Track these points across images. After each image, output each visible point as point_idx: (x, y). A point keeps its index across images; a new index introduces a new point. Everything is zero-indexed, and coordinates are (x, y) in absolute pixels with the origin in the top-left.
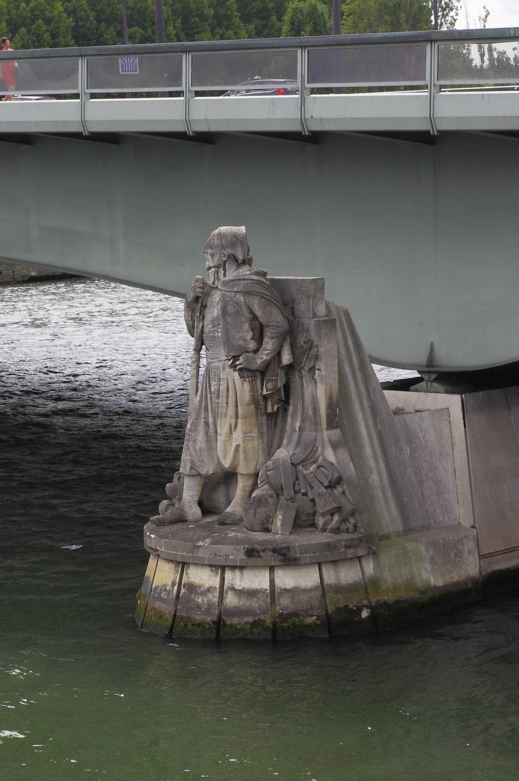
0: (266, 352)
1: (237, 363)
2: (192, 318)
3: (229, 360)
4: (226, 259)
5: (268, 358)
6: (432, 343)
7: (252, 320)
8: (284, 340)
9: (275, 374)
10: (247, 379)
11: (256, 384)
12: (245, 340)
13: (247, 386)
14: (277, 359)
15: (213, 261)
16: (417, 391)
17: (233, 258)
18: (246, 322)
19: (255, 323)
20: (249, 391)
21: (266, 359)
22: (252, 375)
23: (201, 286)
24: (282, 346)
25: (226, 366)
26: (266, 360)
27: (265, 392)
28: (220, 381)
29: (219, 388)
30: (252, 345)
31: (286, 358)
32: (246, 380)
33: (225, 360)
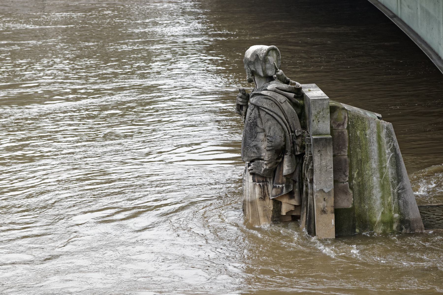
0: (265, 162)
1: (250, 168)
5: (267, 168)
9: (280, 181)
10: (257, 184)
12: (258, 149)
13: (257, 190)
18: (261, 132)
21: (266, 168)
22: (264, 180)
26: (265, 170)
27: (271, 198)
31: (286, 169)
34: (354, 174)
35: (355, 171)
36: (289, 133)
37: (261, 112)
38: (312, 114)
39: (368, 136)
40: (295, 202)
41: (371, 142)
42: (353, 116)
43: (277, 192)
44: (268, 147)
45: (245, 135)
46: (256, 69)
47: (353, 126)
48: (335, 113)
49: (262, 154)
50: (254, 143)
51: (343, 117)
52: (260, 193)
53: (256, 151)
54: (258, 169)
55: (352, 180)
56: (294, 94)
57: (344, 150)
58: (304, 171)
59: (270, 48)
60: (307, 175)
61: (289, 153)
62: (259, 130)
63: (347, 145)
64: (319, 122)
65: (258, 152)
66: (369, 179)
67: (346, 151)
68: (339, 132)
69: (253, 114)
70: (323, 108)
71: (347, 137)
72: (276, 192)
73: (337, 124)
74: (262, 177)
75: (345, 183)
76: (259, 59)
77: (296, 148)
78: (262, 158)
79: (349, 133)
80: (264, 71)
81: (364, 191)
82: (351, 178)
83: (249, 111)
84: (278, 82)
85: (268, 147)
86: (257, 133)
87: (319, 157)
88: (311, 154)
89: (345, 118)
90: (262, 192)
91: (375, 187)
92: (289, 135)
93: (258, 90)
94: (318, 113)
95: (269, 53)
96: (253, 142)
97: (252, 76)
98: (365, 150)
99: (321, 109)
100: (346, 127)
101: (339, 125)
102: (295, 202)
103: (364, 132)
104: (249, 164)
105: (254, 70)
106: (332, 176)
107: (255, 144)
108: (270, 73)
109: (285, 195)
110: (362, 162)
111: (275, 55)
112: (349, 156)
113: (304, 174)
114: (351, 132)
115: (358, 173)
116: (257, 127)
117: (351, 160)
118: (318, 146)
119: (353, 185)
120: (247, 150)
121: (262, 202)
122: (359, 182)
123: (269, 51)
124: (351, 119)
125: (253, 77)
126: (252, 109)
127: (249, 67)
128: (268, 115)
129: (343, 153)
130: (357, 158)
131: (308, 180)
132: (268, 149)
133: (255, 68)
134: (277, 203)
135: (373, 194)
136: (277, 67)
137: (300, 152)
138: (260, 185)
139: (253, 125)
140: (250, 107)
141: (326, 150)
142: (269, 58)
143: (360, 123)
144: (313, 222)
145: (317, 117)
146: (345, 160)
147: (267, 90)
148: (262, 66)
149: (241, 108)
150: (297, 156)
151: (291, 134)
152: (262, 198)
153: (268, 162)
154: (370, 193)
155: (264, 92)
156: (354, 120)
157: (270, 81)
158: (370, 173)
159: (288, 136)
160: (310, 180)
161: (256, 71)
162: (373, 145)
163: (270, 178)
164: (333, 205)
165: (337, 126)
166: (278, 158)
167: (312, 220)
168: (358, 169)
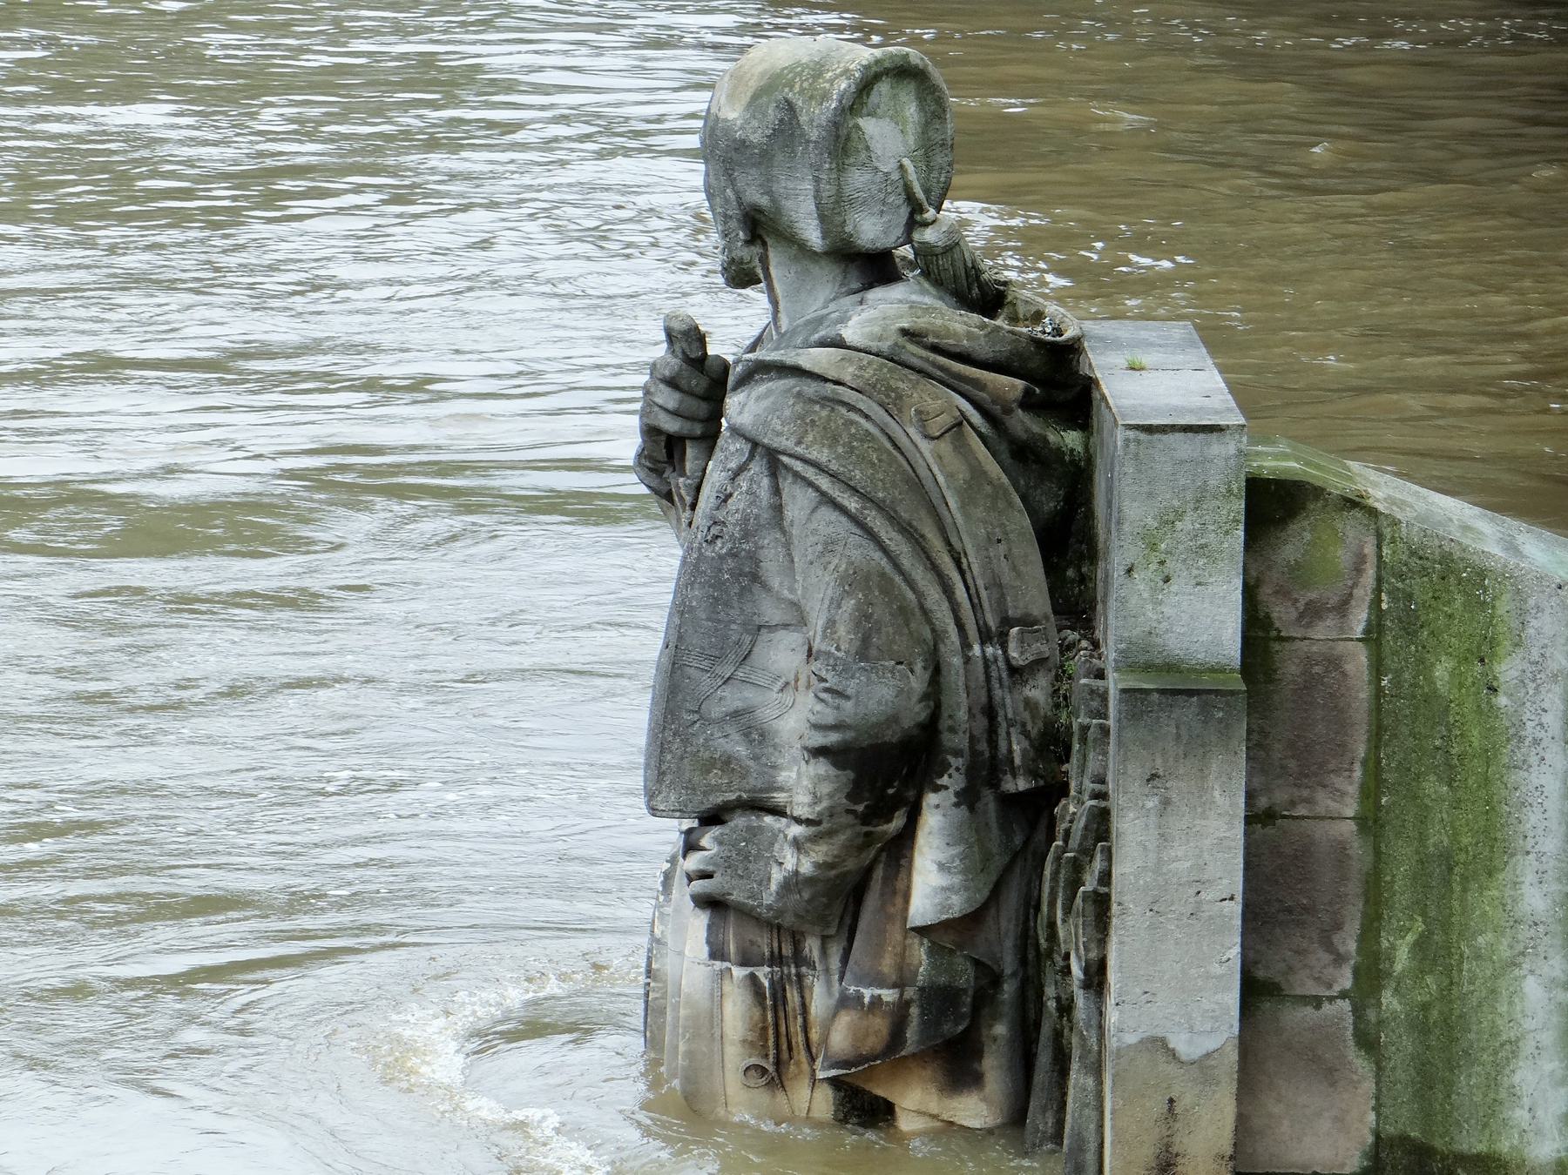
0: (796, 830)
1: (693, 862)
5: (806, 868)
9: (887, 965)
10: (739, 972)
12: (757, 734)
13: (736, 1012)
18: (786, 626)
20: (744, 1041)
21: (796, 873)
22: (787, 950)
26: (793, 883)
34: (1393, 947)
35: (1403, 931)
36: (966, 645)
37: (787, 484)
38: (1126, 527)
39: (1502, 700)
41: (1521, 740)
42: (1413, 553)
43: (867, 1035)
44: (816, 727)
45: (680, 638)
46: (773, 200)
47: (1410, 626)
48: (1294, 527)
50: (733, 698)
51: (1343, 557)
53: (741, 750)
54: (746, 876)
55: (1376, 990)
56: (1020, 384)
57: (1338, 781)
58: (1052, 904)
59: (877, 62)
60: (1072, 934)
61: (953, 781)
62: (771, 612)
63: (1361, 751)
64: (1167, 580)
65: (756, 758)
66: (1493, 991)
67: (1352, 789)
68: (1309, 660)
69: (737, 503)
70: (1204, 488)
71: (1363, 695)
72: (858, 1036)
73: (1301, 605)
74: (773, 926)
75: (1326, 1007)
76: (803, 135)
77: (1010, 751)
79: (1377, 668)
81: (1451, 1071)
82: (1371, 975)
83: (716, 476)
84: (923, 292)
85: (816, 727)
87: (1153, 819)
88: (1102, 796)
89: (1358, 569)
90: (764, 1029)
91: (1528, 1047)
92: (967, 660)
93: (785, 339)
94: (1168, 521)
95: (874, 98)
96: (726, 692)
97: (749, 242)
98: (1482, 793)
99: (1189, 496)
100: (1358, 630)
101: (1313, 612)
102: (983, 1108)
103: (1478, 668)
104: (689, 832)
105: (764, 201)
106: (1237, 949)
107: (739, 704)
108: (871, 230)
109: (914, 1055)
110: (1450, 869)
111: (911, 111)
112: (1370, 823)
113: (1052, 925)
114: (1391, 663)
115: (1420, 946)
116: (756, 588)
117: (1377, 853)
118: (1145, 746)
119: (1380, 1022)
120: (686, 742)
121: (763, 1097)
122: (1425, 1007)
123: (868, 82)
124: (1401, 577)
125: (756, 250)
126: (733, 465)
127: (732, 181)
129: (1325, 803)
130: (1422, 838)
132: (818, 739)
133: (769, 193)
135: (1513, 1094)
136: (920, 194)
137: (1033, 773)
138: (753, 978)
139: (737, 574)
140: (730, 450)
141: (1202, 774)
142: (868, 125)
143: (1458, 604)
145: (1153, 547)
146: (1341, 848)
147: (839, 343)
148: (817, 180)
149: (670, 455)
150: (1009, 802)
151: (977, 649)
152: (764, 1071)
154: (1493, 1082)
156: (1417, 585)
157: (869, 286)
158: (1504, 951)
159: (957, 661)
160: (1086, 971)
161: (778, 210)
162: (1533, 760)
164: (1229, 1151)
165: (1301, 616)
166: (880, 811)
168: (1424, 914)
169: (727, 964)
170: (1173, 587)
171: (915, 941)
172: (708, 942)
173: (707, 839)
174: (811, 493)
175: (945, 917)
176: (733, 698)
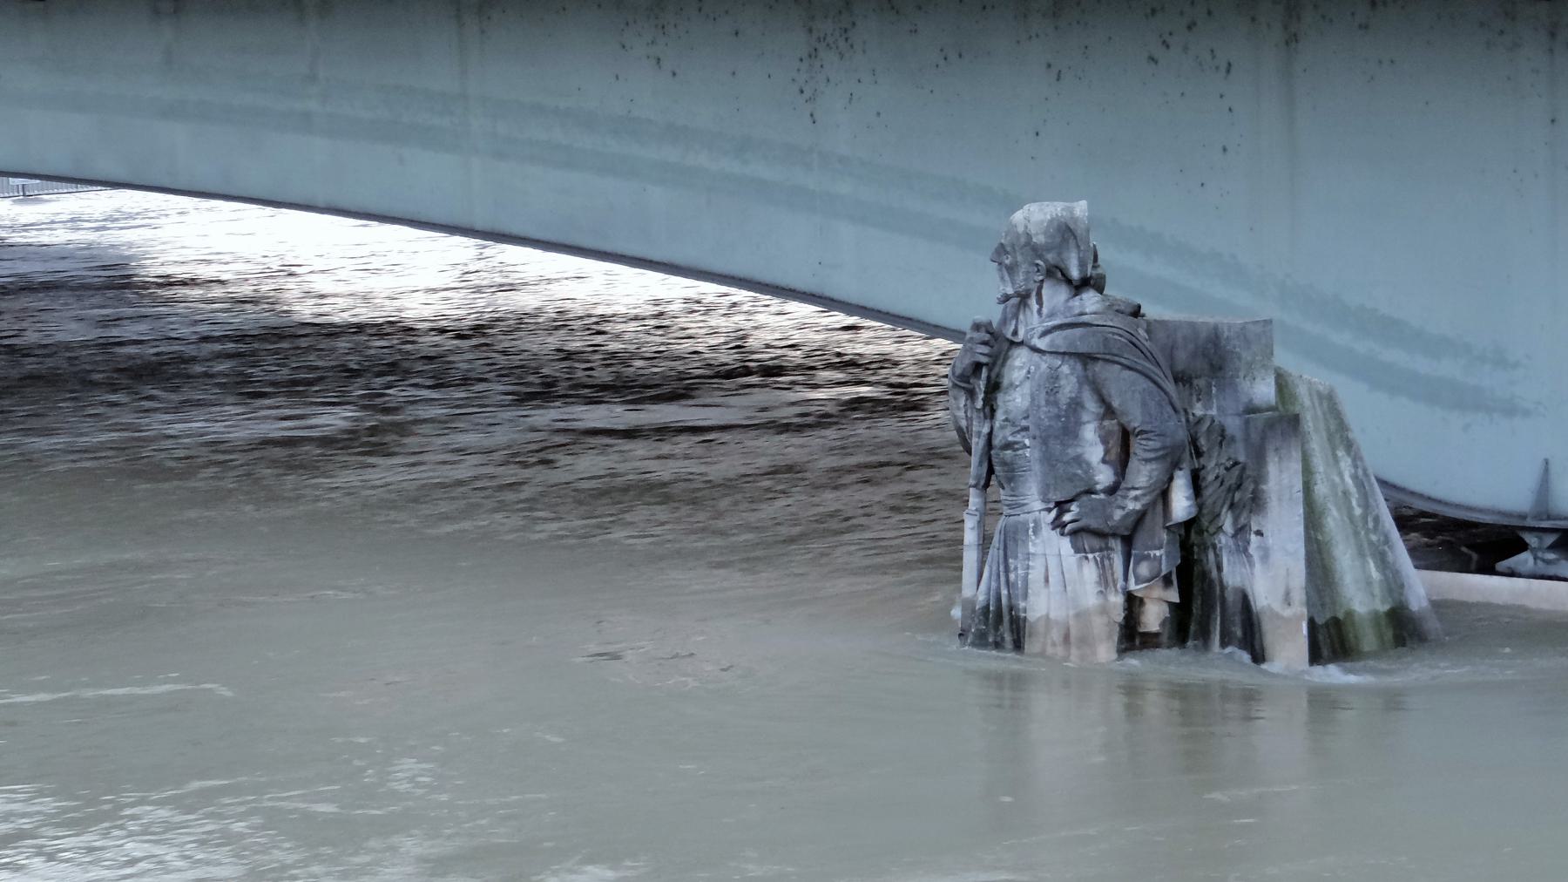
0: (1133, 493)
1: (1067, 517)
2: (966, 412)
3: (1049, 510)
4: (1041, 278)
5: (1138, 506)
6: (1547, 462)
7: (1103, 418)
8: (1176, 465)
9: (1157, 541)
10: (1090, 556)
11: (1111, 566)
13: (1090, 572)
14: (1160, 507)
15: (1013, 283)
16: (1512, 574)
17: (1056, 272)
18: (1088, 422)
19: (1110, 424)
22: (1103, 545)
23: (986, 339)
24: (1171, 479)
25: (1043, 525)
27: (1132, 586)
28: (1028, 559)
29: (1027, 574)
30: (1104, 477)
31: (1181, 504)
32: (1087, 558)
33: (1040, 511)
40: (1174, 596)
49: (1097, 478)
50: (1071, 452)
52: (1098, 579)
58: (1222, 507)
62: (1085, 417)
64: (1254, 379)
78: (1099, 487)
80: (1082, 265)
86: (1079, 423)
87: (1277, 465)
88: (1236, 463)
91: (1333, 542)
96: (1070, 451)
106: (1301, 511)
113: (1218, 515)
116: (1079, 409)
128: (1131, 373)
131: (1228, 526)
134: (1133, 603)
135: (1333, 557)
144: (1257, 636)
152: (1101, 592)
153: (1148, 490)
155: (1085, 318)
163: (1114, 535)
167: (1256, 629)
169: (1084, 554)
170: (1256, 380)
171: (1162, 531)
172: (1072, 547)
173: (1074, 507)
174: (1119, 366)
175: (1190, 517)
176: (1071, 452)
